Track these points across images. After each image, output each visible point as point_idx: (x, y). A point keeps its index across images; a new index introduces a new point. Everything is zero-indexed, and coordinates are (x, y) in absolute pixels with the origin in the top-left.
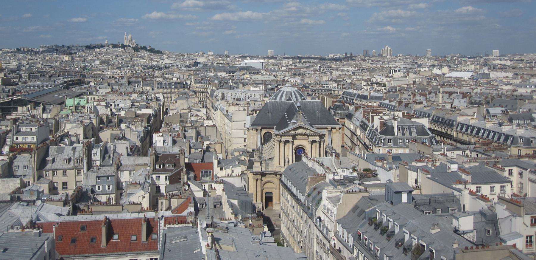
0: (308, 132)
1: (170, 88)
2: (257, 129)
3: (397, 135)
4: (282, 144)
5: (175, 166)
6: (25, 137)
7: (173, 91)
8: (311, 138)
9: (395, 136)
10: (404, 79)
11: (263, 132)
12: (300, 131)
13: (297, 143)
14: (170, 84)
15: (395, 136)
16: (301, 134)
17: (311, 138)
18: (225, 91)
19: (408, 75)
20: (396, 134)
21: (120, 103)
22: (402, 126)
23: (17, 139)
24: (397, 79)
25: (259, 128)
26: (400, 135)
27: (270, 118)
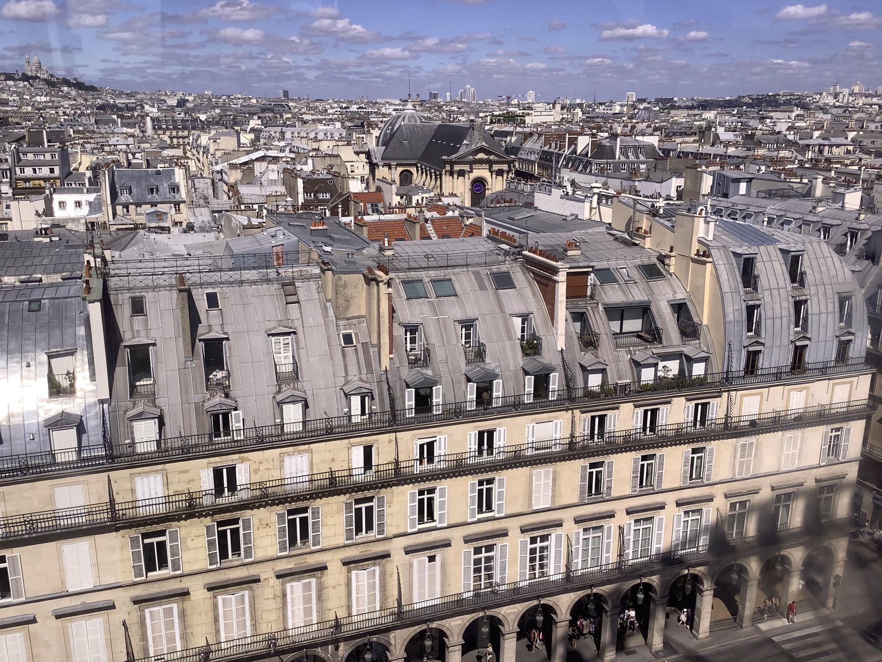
0: (492, 157)
1: (175, 128)
2: (390, 168)
3: (619, 158)
4: (455, 176)
5: (331, 195)
6: (37, 168)
7: (180, 133)
8: (496, 167)
9: (617, 160)
10: (548, 113)
11: (400, 169)
12: (481, 156)
13: (473, 176)
14: (174, 121)
15: (617, 160)
16: (481, 162)
17: (496, 167)
18: (284, 129)
19: (554, 108)
20: (617, 157)
21: (118, 143)
22: (625, 146)
23: (22, 171)
24: (539, 113)
25: (394, 163)
26: (623, 159)
27: (408, 149)
